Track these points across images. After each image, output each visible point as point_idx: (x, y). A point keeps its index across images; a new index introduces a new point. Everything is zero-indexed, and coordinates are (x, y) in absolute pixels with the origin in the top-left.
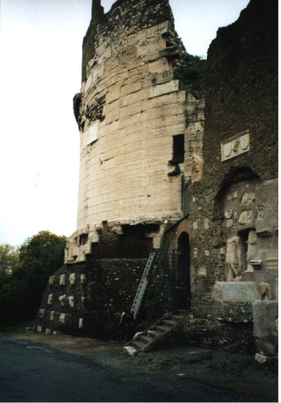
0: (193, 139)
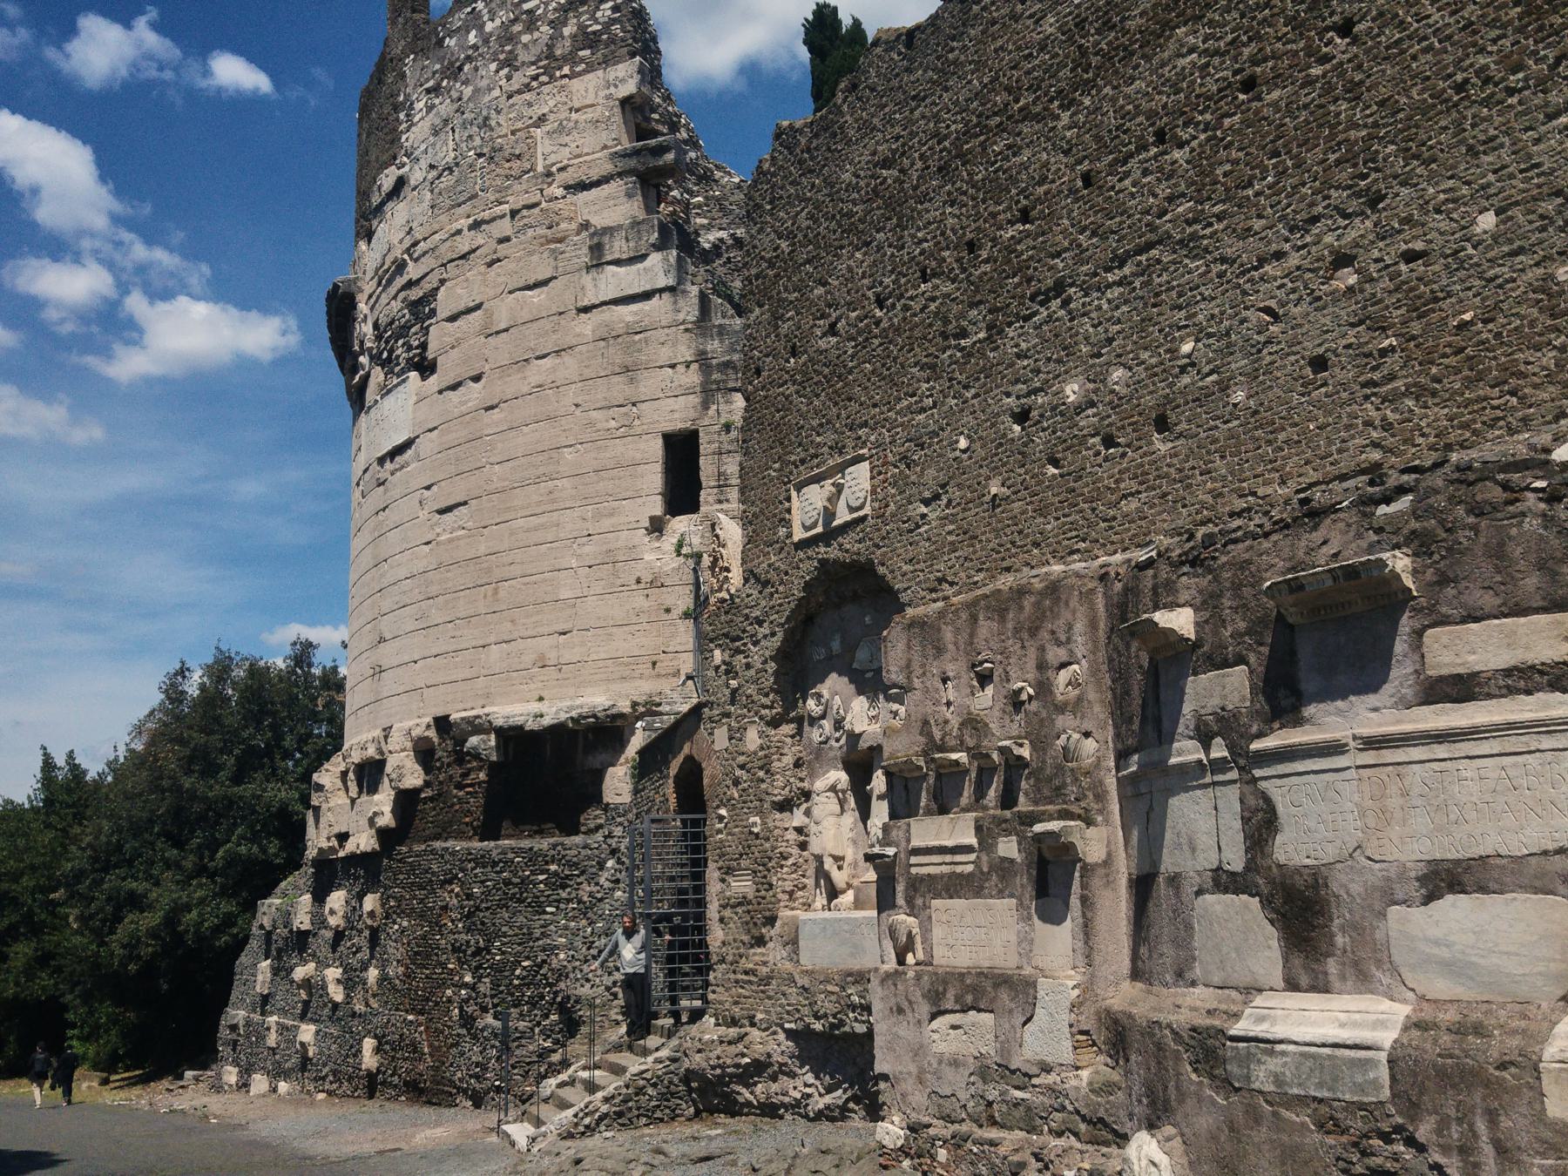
0: (726, 447)
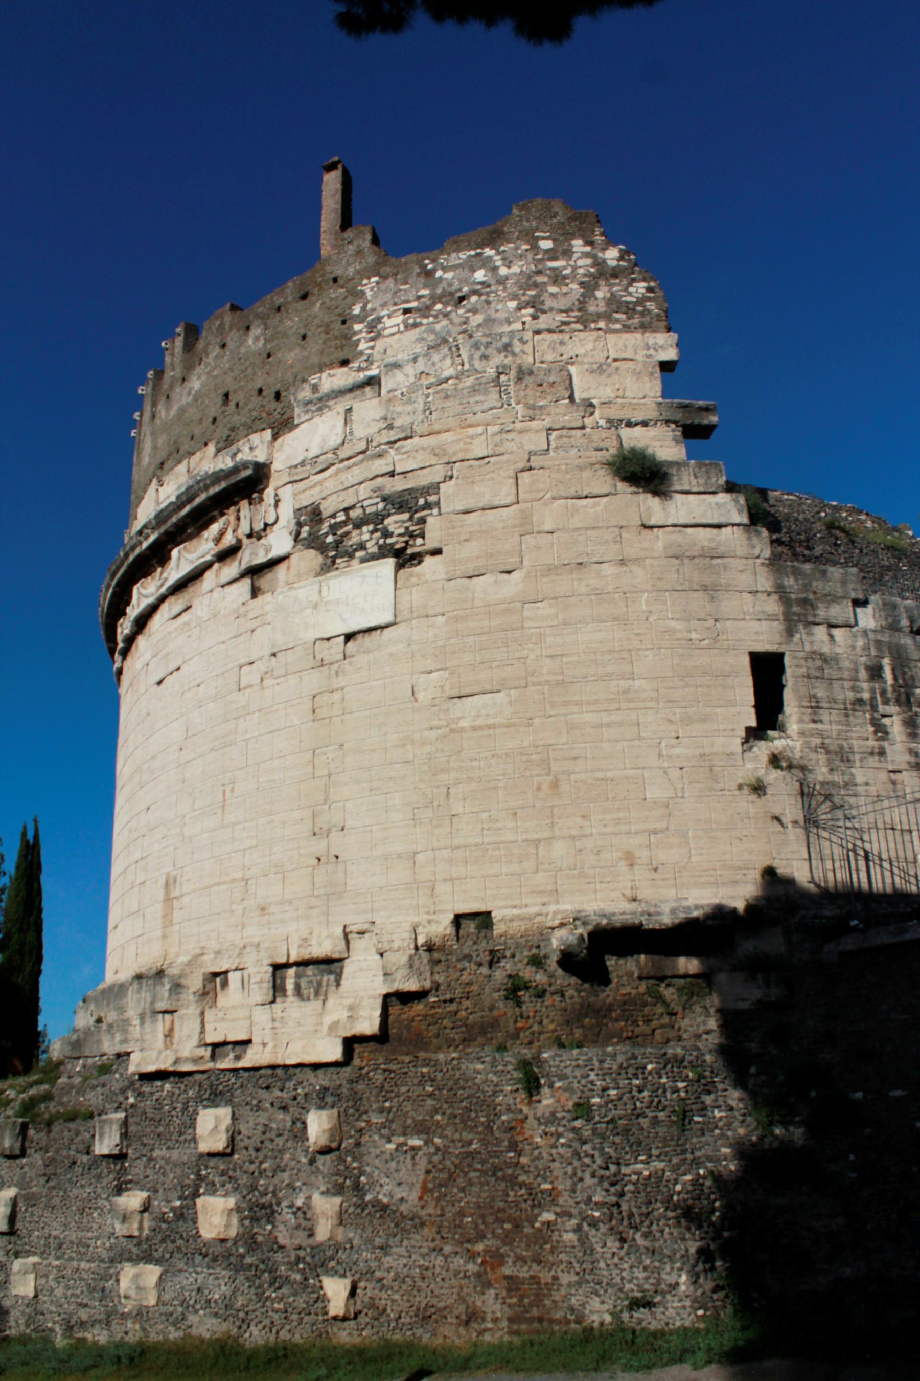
0: (813, 672)
